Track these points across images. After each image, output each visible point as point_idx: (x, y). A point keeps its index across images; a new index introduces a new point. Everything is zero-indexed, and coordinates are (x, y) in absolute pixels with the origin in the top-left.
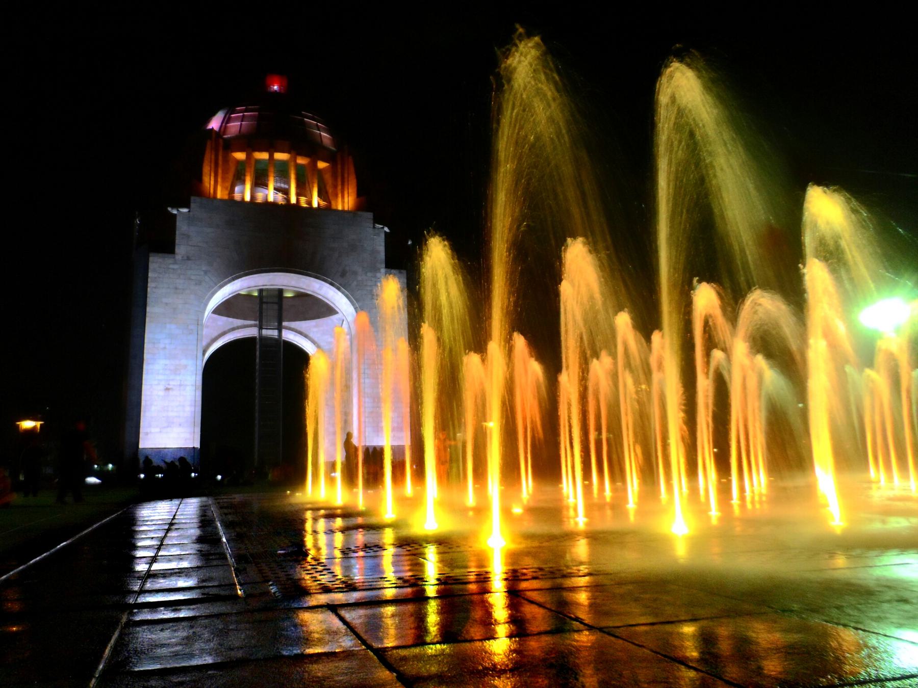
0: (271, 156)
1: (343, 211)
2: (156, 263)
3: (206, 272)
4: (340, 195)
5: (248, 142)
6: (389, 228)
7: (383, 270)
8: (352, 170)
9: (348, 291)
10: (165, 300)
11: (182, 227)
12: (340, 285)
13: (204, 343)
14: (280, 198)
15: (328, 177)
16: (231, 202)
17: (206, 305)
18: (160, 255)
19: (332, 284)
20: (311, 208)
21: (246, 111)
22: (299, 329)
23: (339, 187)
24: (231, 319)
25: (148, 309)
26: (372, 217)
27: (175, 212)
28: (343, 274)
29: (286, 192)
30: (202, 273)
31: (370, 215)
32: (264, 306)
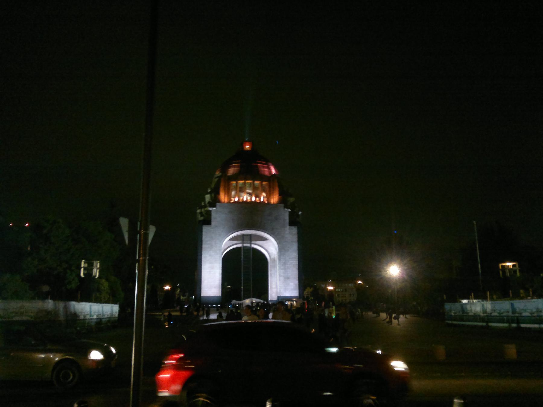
2: (205, 229)
5: (236, 177)
7: (288, 227)
8: (276, 184)
10: (209, 242)
11: (214, 215)
13: (222, 251)
15: (267, 187)
17: (223, 243)
19: (268, 234)
21: (235, 163)
22: (259, 244)
26: (283, 206)
27: (210, 209)
28: (273, 229)
31: (282, 205)
32: (245, 237)
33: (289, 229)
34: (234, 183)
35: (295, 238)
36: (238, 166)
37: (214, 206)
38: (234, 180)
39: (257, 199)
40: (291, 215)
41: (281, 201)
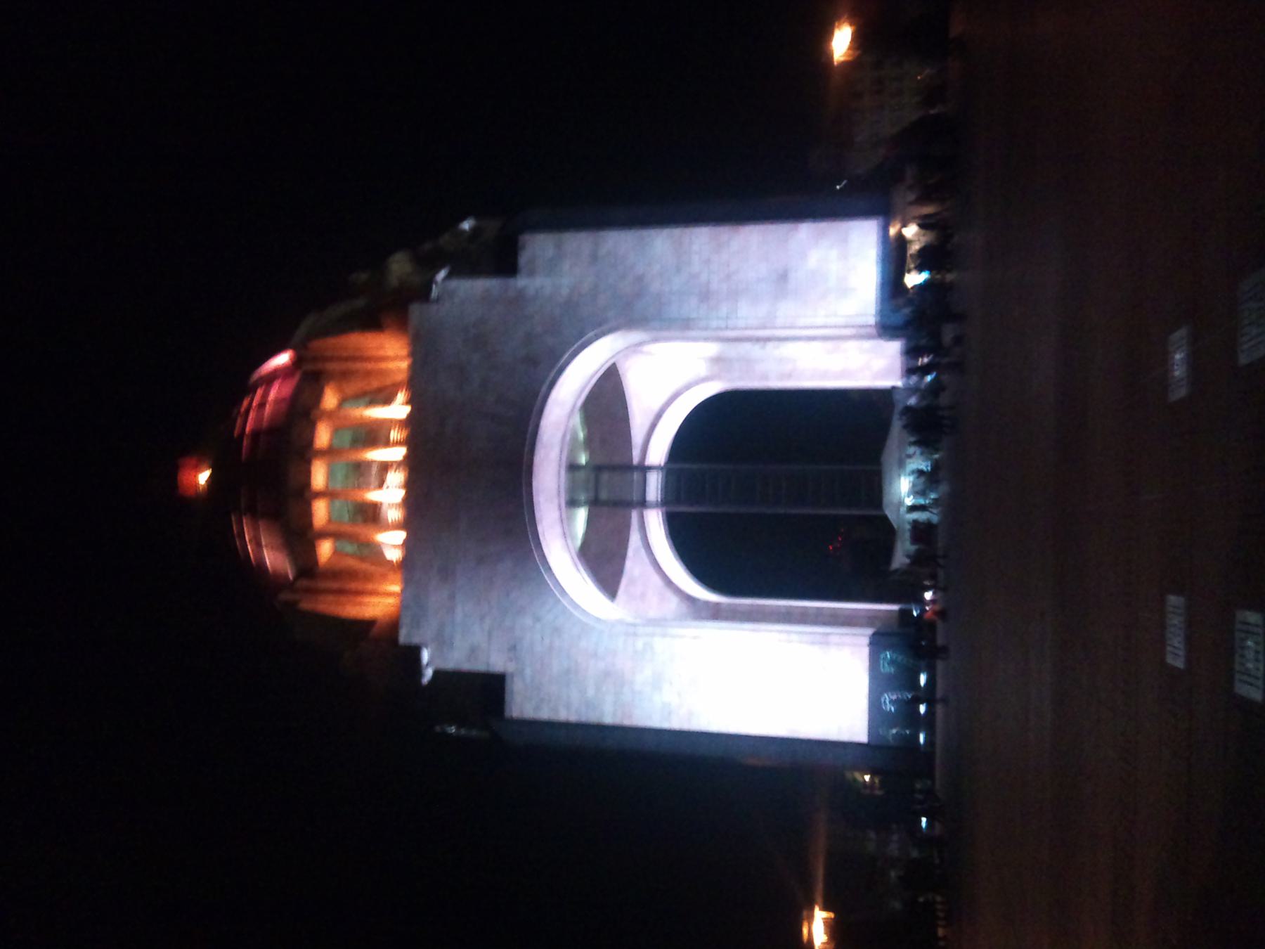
0: (319, 495)
1: (412, 354)
3: (537, 619)
4: (383, 365)
6: (437, 272)
7: (521, 282)
9: (564, 353)
10: (591, 692)
11: (457, 660)
12: (552, 367)
14: (396, 479)
15: (353, 387)
16: (406, 565)
18: (507, 698)
20: (409, 422)
23: (369, 366)
24: (630, 553)
25: (608, 719)
27: (429, 673)
29: (385, 467)
30: (538, 626)
31: (415, 310)
32: (604, 495)
33: (532, 273)
34: (325, 549)
35: (578, 243)
36: (256, 529)
37: (415, 651)
38: (312, 550)
39: (395, 435)
40: (466, 266)
41: (402, 324)
